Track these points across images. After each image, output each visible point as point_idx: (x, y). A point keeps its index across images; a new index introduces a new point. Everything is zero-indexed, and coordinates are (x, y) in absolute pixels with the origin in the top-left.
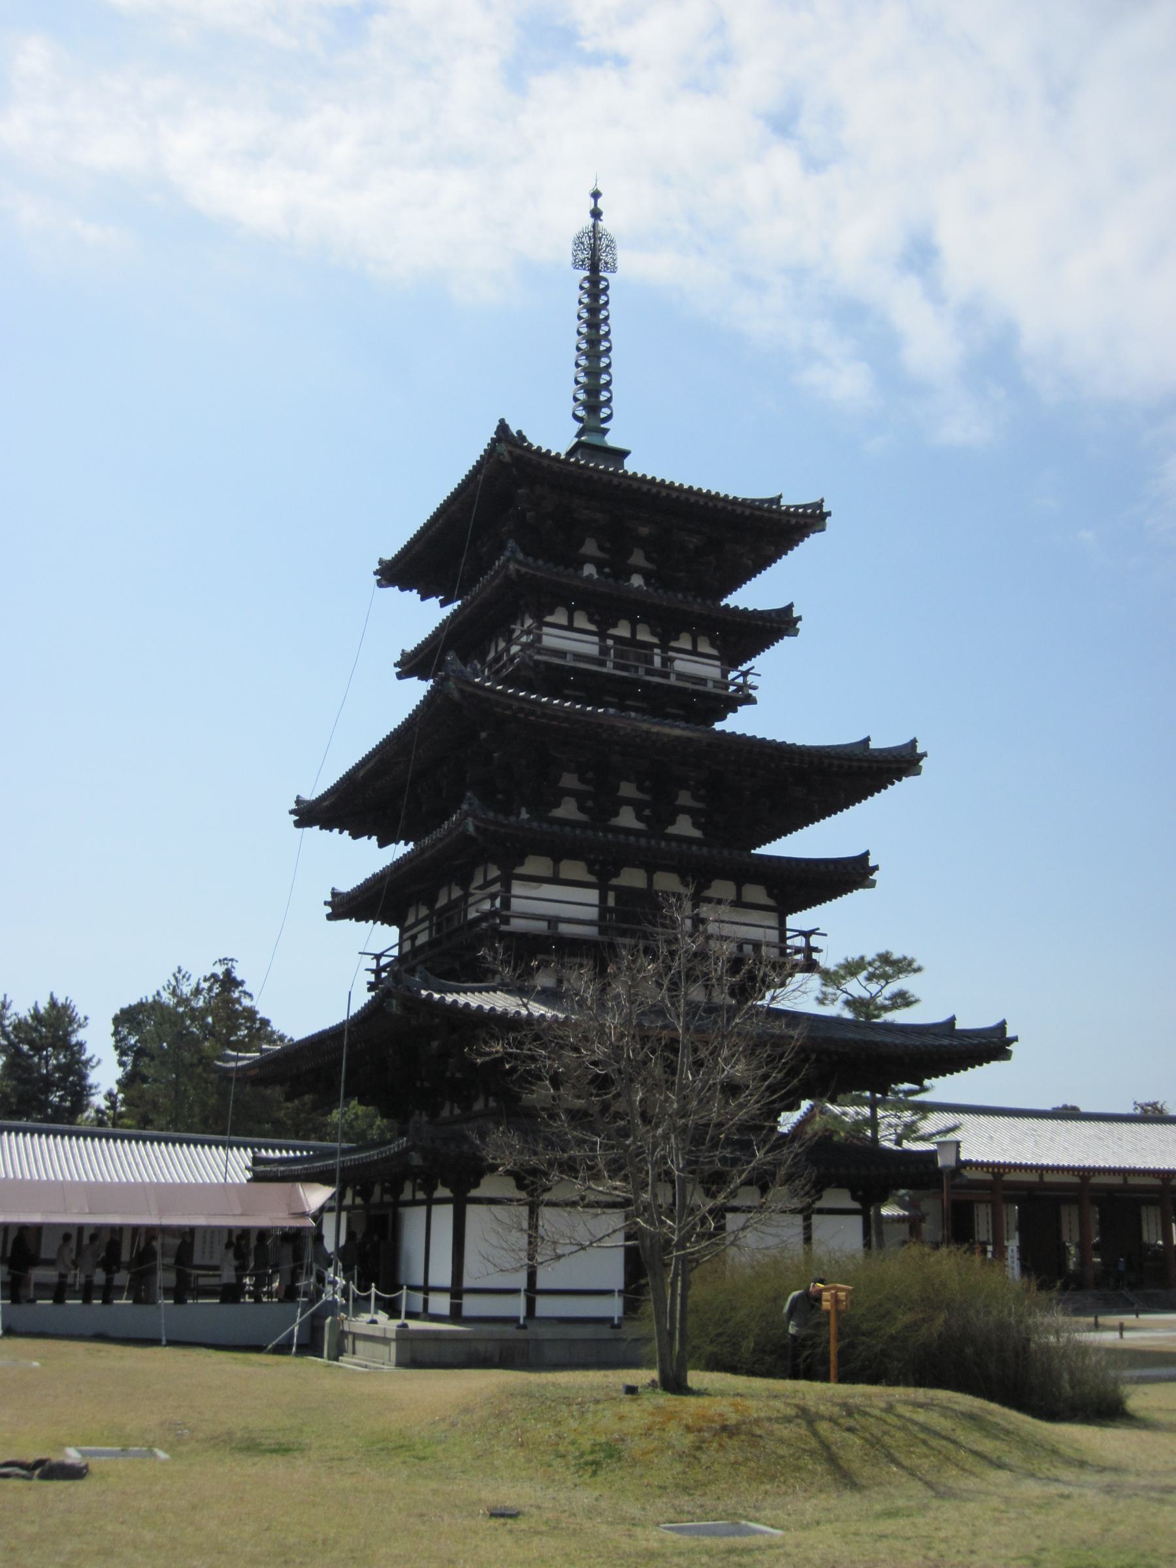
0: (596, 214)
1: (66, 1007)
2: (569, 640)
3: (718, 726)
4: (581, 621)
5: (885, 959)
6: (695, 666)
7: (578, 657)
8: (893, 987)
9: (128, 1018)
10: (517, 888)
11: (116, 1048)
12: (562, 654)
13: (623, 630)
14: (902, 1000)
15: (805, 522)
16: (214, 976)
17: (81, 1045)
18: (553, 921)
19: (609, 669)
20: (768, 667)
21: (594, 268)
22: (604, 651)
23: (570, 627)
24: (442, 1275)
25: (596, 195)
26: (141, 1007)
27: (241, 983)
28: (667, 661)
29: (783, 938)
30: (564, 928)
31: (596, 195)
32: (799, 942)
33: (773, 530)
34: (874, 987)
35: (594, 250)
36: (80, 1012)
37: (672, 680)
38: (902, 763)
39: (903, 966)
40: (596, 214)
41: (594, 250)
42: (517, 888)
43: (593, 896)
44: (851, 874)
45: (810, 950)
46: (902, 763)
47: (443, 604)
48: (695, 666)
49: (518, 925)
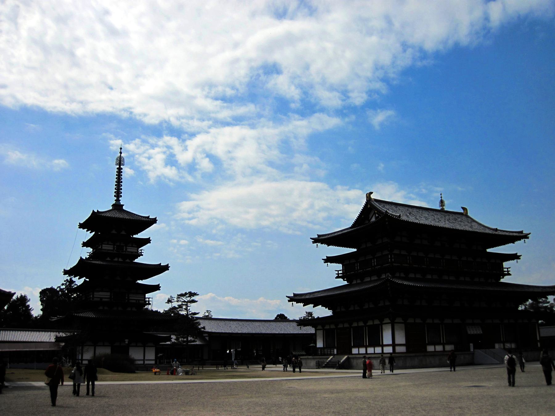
0: (121, 153)
1: (25, 296)
2: (107, 247)
3: (136, 261)
4: (110, 243)
5: (190, 293)
6: (131, 249)
7: (108, 250)
8: (193, 298)
9: (43, 293)
10: (95, 293)
11: (41, 300)
12: (105, 250)
13: (118, 244)
14: (193, 301)
15: (154, 221)
16: (67, 280)
17: (29, 306)
18: (101, 298)
19: (115, 252)
20: (144, 249)
21: (120, 164)
22: (114, 248)
23: (108, 244)
24: (80, 358)
25: (121, 149)
26: (47, 289)
27: (75, 282)
28: (126, 249)
29: (145, 298)
30: (104, 300)
31: (121, 149)
32: (148, 300)
33: (149, 222)
34: (188, 299)
35: (120, 161)
36: (28, 298)
37: (127, 253)
38: (166, 268)
39: (195, 294)
40: (121, 153)
41: (120, 161)
42: (95, 293)
43: (109, 294)
44: (156, 288)
45: (149, 301)
46: (166, 268)
47: (90, 233)
48: (131, 249)
49: (95, 299)
